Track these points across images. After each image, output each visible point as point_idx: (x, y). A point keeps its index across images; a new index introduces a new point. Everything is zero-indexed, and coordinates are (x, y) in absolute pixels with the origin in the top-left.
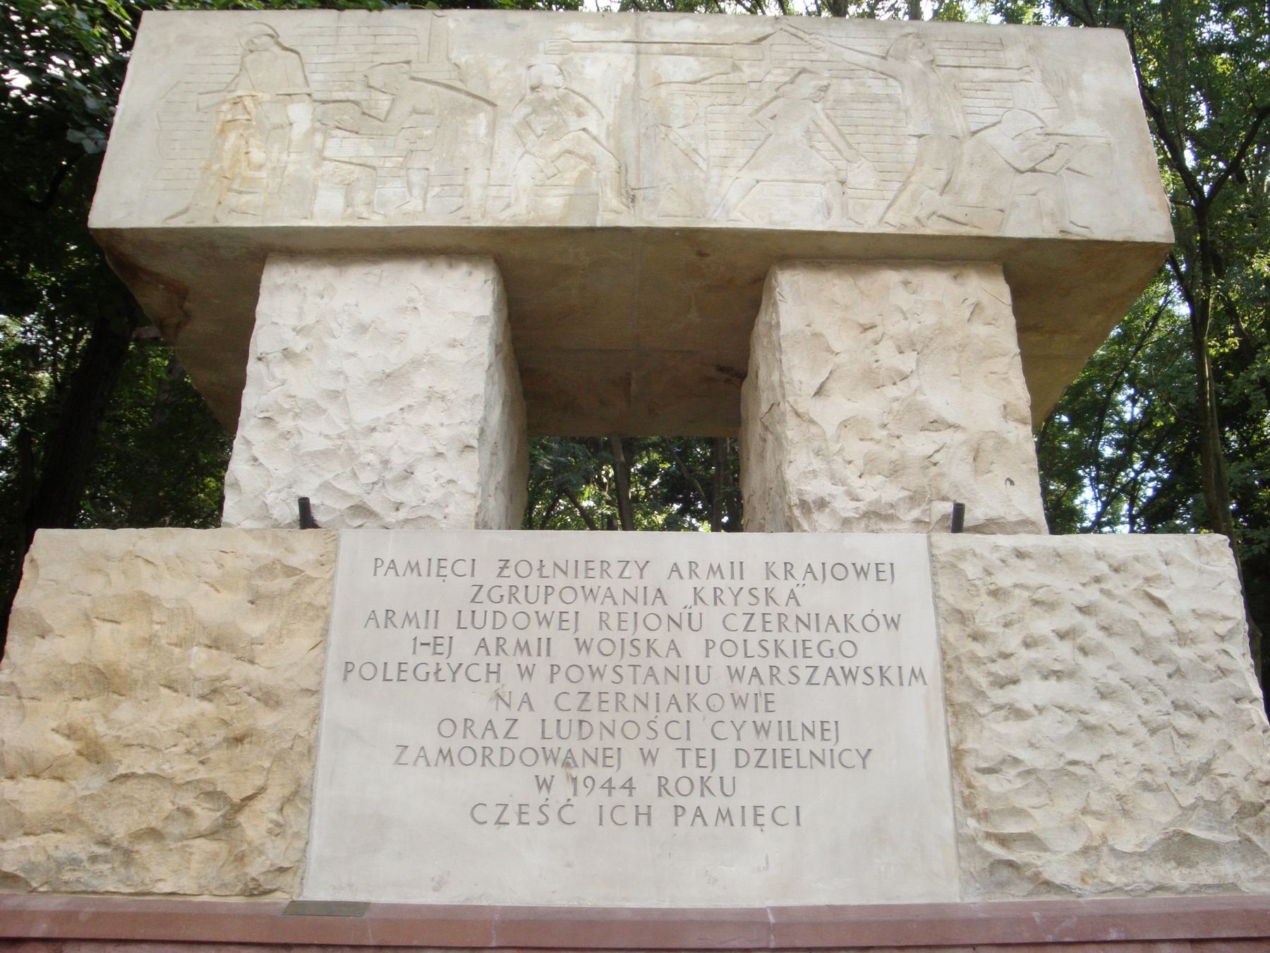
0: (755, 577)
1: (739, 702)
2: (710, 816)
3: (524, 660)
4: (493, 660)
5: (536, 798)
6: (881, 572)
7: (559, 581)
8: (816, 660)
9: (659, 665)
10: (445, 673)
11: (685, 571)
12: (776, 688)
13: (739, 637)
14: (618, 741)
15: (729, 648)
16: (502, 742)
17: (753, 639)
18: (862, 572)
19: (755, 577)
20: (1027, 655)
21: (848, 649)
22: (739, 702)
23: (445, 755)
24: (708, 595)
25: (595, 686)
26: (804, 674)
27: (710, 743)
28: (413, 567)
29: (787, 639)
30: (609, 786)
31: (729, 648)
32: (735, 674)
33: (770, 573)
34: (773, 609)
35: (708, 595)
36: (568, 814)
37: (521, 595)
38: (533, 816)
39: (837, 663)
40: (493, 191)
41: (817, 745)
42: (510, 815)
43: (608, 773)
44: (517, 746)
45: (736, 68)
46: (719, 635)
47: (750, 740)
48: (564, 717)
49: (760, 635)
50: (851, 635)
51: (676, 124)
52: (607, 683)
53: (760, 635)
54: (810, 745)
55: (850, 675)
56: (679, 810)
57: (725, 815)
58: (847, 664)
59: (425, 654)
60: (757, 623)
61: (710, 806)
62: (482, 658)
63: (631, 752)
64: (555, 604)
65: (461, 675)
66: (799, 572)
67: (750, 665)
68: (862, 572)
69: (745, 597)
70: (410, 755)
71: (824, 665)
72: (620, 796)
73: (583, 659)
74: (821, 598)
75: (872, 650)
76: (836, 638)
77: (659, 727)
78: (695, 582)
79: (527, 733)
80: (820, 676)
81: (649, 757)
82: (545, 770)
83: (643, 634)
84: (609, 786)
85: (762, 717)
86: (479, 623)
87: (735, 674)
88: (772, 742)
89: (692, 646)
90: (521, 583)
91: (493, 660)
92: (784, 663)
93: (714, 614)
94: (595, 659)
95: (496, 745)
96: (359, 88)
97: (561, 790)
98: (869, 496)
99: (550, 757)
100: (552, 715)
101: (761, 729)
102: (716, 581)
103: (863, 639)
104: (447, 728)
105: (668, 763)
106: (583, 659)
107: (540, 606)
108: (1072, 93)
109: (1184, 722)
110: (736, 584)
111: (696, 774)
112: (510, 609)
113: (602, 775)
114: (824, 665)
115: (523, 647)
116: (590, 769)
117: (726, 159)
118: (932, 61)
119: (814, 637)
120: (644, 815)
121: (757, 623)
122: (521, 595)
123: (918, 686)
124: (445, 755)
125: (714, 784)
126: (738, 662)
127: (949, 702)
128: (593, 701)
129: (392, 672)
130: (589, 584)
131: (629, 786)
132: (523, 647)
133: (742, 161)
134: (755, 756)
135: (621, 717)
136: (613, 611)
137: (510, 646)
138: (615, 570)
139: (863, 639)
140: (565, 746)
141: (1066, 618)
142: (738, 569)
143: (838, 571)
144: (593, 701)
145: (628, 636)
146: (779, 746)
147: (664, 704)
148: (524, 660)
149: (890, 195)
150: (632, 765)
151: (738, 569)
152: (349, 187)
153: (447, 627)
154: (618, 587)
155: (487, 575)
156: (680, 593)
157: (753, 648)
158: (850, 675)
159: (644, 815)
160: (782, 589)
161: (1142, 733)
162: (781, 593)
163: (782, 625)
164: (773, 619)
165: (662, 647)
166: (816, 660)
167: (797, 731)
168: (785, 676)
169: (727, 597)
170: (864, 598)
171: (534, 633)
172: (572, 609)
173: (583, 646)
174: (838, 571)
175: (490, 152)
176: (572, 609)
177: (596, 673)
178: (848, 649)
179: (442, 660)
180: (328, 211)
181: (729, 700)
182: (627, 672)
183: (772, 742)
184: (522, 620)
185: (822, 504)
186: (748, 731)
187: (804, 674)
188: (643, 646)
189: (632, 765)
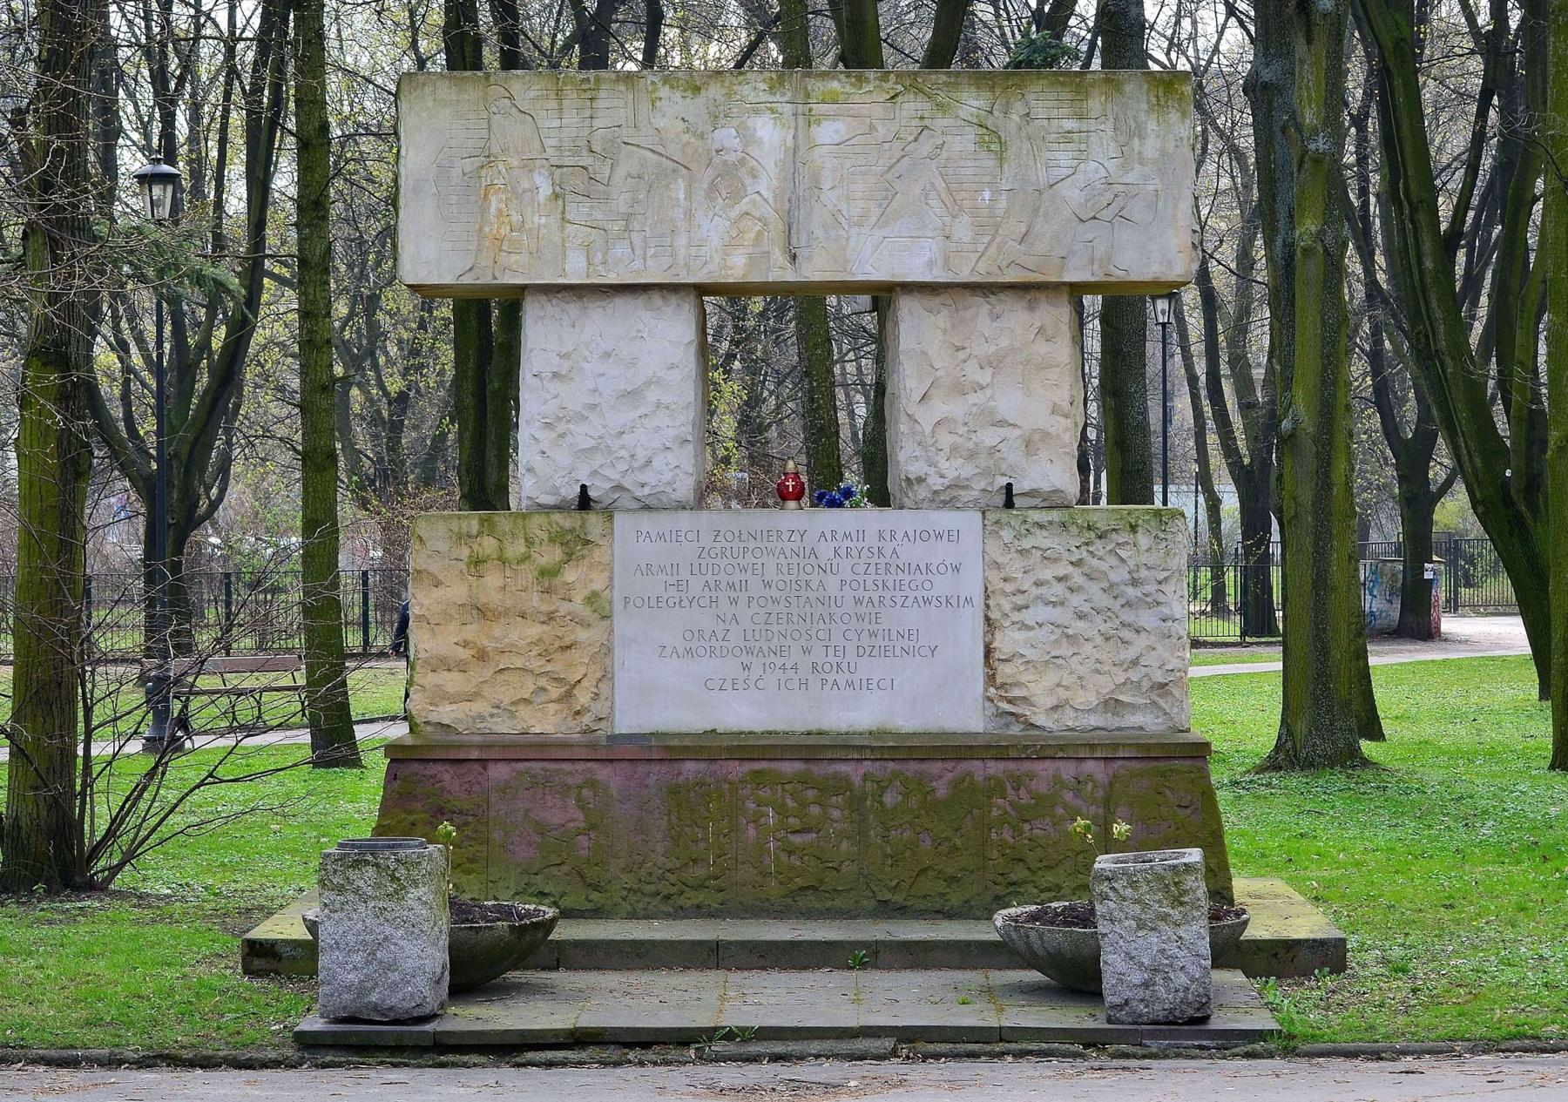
0: (872, 540)
1: (860, 618)
2: (842, 684)
3: (733, 595)
4: (714, 594)
5: (742, 675)
6: (952, 536)
7: (751, 544)
8: (908, 592)
9: (812, 595)
10: (685, 603)
11: (829, 537)
12: (883, 610)
13: (860, 578)
14: (789, 642)
15: (854, 585)
16: (721, 643)
17: (869, 580)
18: (939, 536)
19: (872, 540)
20: (1035, 591)
21: (927, 585)
22: (860, 618)
23: (689, 651)
24: (843, 552)
25: (775, 609)
26: (900, 601)
27: (842, 642)
28: (661, 536)
29: (890, 579)
30: (783, 668)
31: (854, 585)
32: (858, 602)
33: (881, 537)
34: (882, 560)
35: (843, 552)
36: (760, 684)
37: (728, 553)
38: (741, 685)
39: (919, 594)
40: (693, 251)
41: (905, 643)
42: (728, 685)
43: (783, 660)
44: (730, 645)
45: (872, 128)
46: (848, 576)
47: (866, 641)
48: (757, 628)
49: (874, 577)
50: (930, 576)
51: (826, 185)
52: (782, 608)
53: (874, 577)
54: (900, 643)
55: (927, 601)
56: (824, 682)
57: (850, 684)
58: (926, 594)
59: (672, 591)
60: (872, 569)
61: (842, 679)
62: (707, 592)
63: (796, 647)
64: (749, 559)
65: (695, 603)
66: (899, 537)
67: (867, 595)
68: (939, 536)
69: (865, 553)
70: (668, 651)
71: (912, 595)
72: (790, 673)
73: (767, 593)
74: (912, 553)
75: (942, 585)
76: (920, 578)
77: (813, 633)
78: (835, 544)
79: (735, 637)
80: (909, 602)
81: (806, 651)
82: (746, 659)
83: (803, 577)
84: (783, 668)
85: (873, 627)
86: (704, 570)
87: (858, 602)
88: (879, 642)
89: (832, 583)
90: (728, 545)
91: (714, 594)
92: (887, 594)
93: (846, 564)
94: (774, 593)
95: (718, 645)
96: (585, 153)
97: (757, 671)
98: (951, 474)
99: (750, 652)
100: (750, 627)
101: (873, 634)
102: (848, 543)
103: (937, 579)
104: (688, 636)
105: (818, 655)
106: (767, 593)
107: (740, 560)
108: (1136, 141)
109: (1126, 634)
110: (860, 545)
111: (834, 661)
112: (723, 562)
113: (779, 661)
114: (912, 595)
115: (732, 586)
116: (773, 658)
117: (864, 216)
118: (1028, 115)
119: (907, 578)
120: (804, 684)
121: (872, 569)
122: (728, 553)
123: (968, 608)
124: (689, 651)
125: (844, 666)
126: (860, 593)
127: (987, 619)
128: (774, 618)
129: (653, 603)
130: (770, 545)
131: (795, 667)
132: (732, 586)
133: (873, 219)
134: (868, 650)
135: (790, 627)
136: (785, 562)
137: (723, 586)
138: (785, 536)
139: (937, 579)
140: (758, 645)
141: (1063, 569)
142: (861, 534)
143: (923, 536)
144: (774, 618)
145: (793, 578)
146: (883, 644)
147: (816, 618)
148: (733, 595)
149: (981, 248)
150: (795, 656)
151: (861, 534)
152: (588, 249)
153: (685, 574)
154: (788, 546)
155: (706, 541)
156: (826, 551)
157: (870, 585)
158: (927, 601)
159: (804, 684)
160: (888, 548)
161: (1099, 640)
162: (888, 552)
163: (887, 571)
164: (882, 567)
165: (814, 585)
166: (908, 592)
167: (894, 635)
168: (887, 602)
169: (855, 553)
170: (941, 552)
171: (737, 577)
172: (760, 562)
173: (768, 585)
174: (923, 536)
175: (689, 215)
176: (760, 562)
177: (776, 601)
178: (927, 585)
179: (683, 595)
180: (575, 271)
181: (854, 619)
182: (793, 600)
183: (879, 642)
184: (730, 569)
185: (920, 480)
186: (865, 634)
187: (900, 601)
188: (803, 584)
189: (795, 656)
